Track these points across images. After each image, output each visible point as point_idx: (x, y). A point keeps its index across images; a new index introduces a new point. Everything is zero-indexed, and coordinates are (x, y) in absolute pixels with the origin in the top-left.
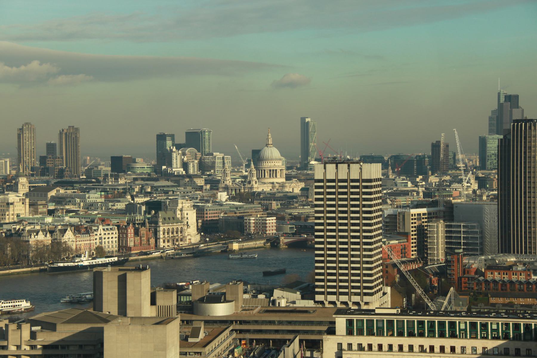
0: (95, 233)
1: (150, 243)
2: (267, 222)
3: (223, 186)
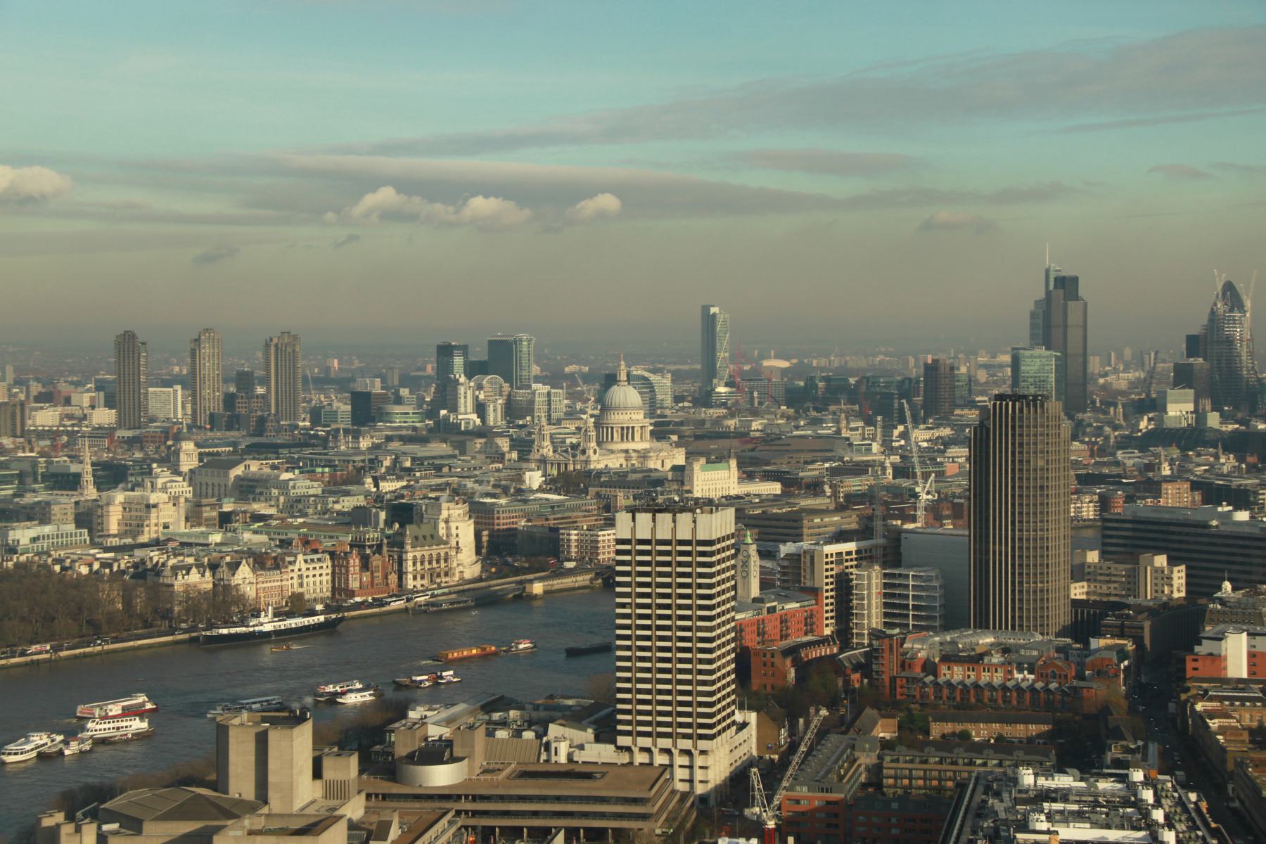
0: (291, 567)
1: (389, 581)
2: (599, 539)
3: (537, 457)
